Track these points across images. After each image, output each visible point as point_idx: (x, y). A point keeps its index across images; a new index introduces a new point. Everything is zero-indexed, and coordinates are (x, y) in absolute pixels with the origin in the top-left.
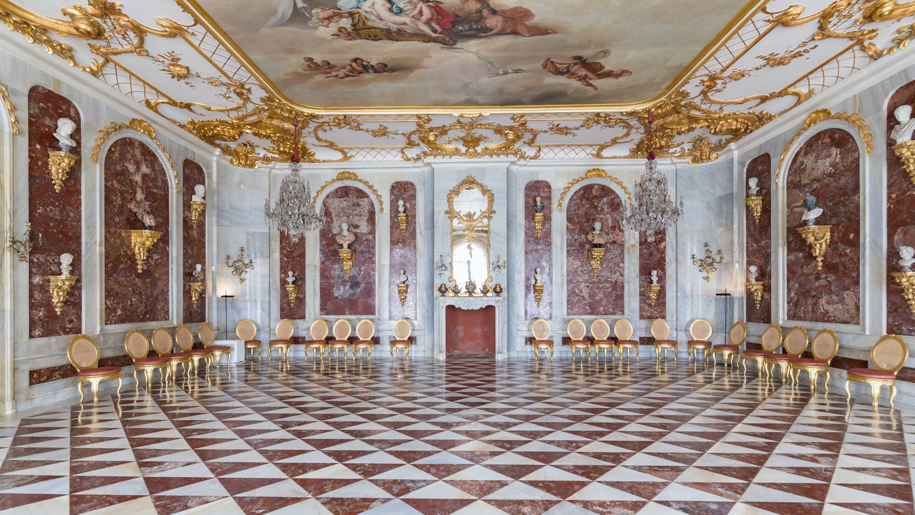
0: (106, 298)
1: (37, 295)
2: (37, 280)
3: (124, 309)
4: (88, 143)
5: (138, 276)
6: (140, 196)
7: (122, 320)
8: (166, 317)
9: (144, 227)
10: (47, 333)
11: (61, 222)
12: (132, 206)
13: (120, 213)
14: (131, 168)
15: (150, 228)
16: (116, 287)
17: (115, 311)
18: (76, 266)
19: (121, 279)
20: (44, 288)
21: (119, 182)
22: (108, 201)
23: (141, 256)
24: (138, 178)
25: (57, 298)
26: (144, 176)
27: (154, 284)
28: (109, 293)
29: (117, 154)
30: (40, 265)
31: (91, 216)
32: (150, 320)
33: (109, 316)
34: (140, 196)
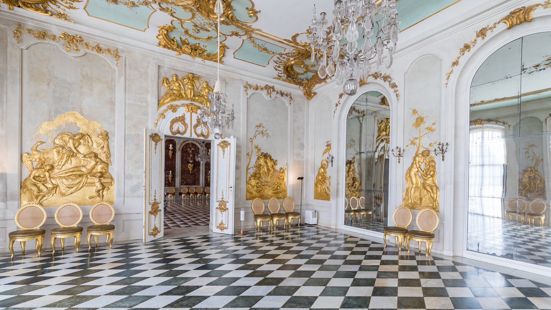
0: (181, 179)
1: (166, 179)
2: (167, 176)
3: (186, 182)
4: (178, 147)
5: (190, 174)
6: (191, 156)
7: (186, 185)
8: (199, 184)
9: (190, 163)
10: (168, 186)
11: (171, 164)
12: (189, 158)
13: (185, 161)
14: (189, 150)
15: (192, 163)
16: (184, 177)
17: (184, 182)
18: (174, 173)
19: (186, 175)
20: (168, 177)
21: (186, 154)
22: (182, 158)
23: (191, 169)
24: (191, 152)
25: (170, 179)
26: (192, 151)
27: (195, 176)
28: (182, 178)
29: (185, 148)
30: (167, 173)
31: (178, 162)
32: (194, 185)
33: (182, 183)
34: (191, 156)
